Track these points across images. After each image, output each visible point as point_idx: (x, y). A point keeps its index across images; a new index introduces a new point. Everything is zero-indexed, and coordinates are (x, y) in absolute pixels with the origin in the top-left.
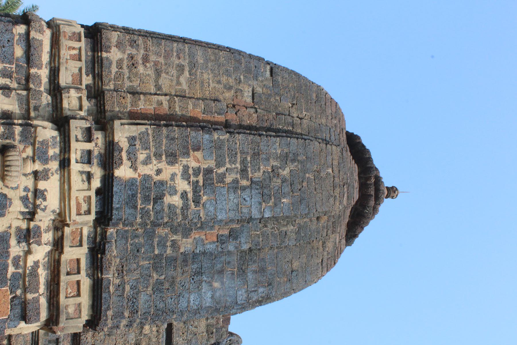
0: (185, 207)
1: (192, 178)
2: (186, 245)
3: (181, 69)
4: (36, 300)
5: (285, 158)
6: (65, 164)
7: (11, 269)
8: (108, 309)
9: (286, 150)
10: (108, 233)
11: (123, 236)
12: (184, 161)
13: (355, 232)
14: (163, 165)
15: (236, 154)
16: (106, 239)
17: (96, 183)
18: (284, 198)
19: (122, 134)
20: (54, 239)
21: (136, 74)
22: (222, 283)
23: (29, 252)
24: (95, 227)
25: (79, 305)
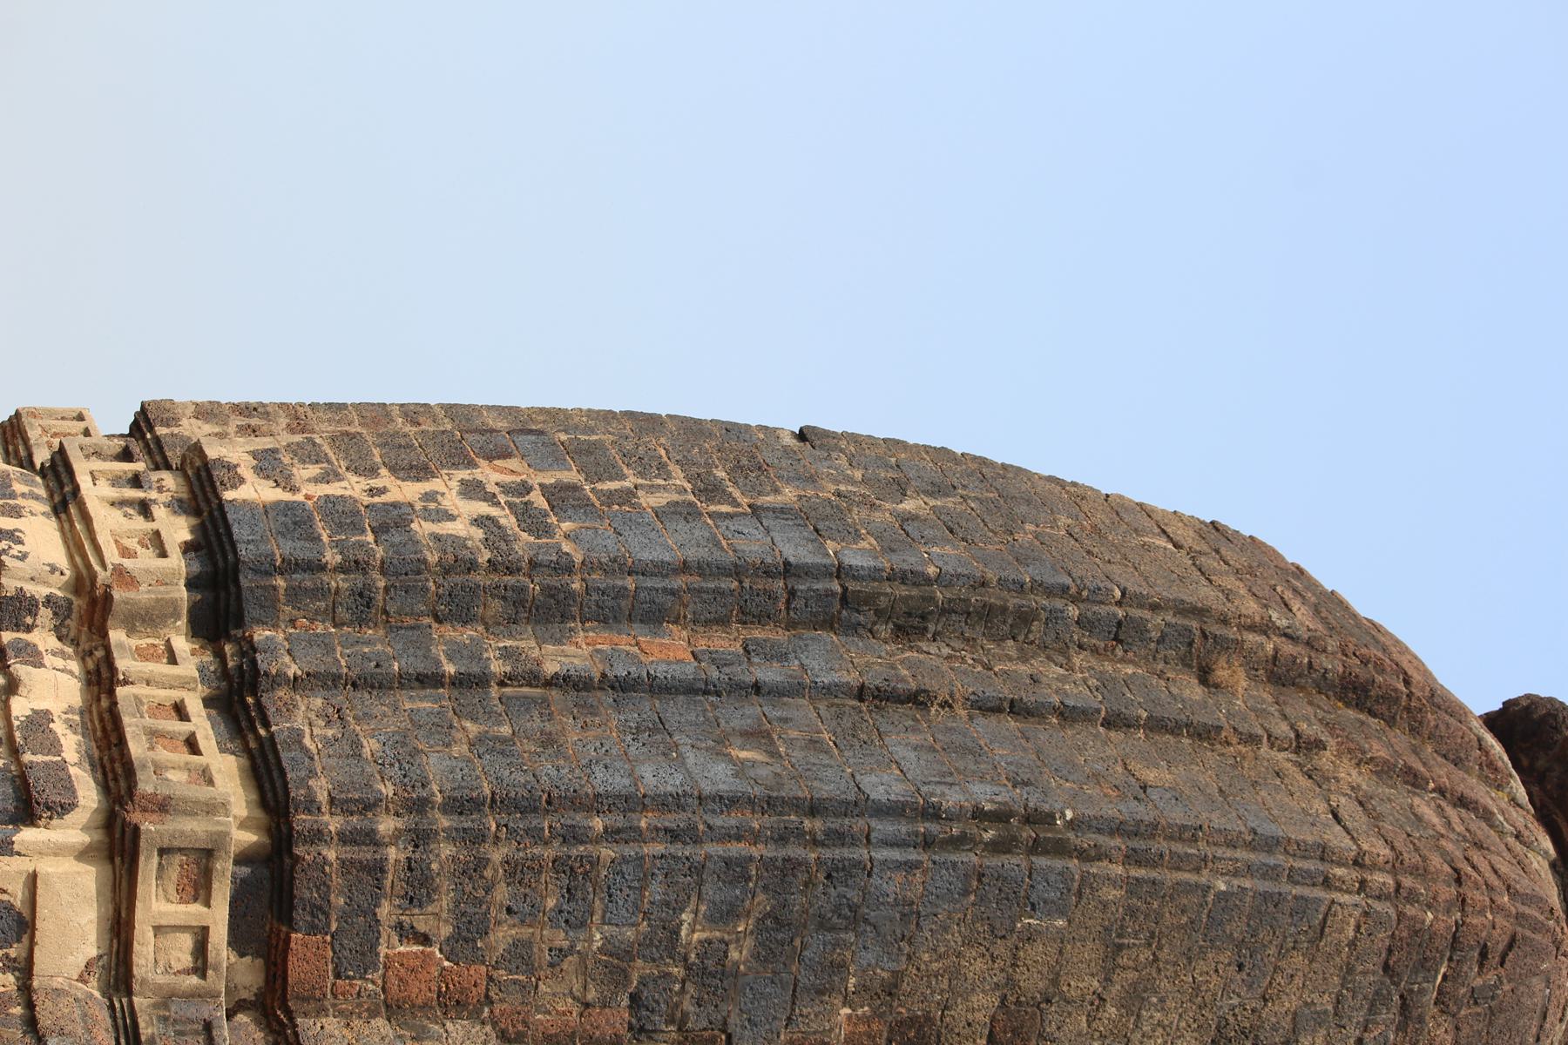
1: (502, 499)
8: (312, 773)
10: (256, 638)
12: (464, 474)
14: (385, 479)
15: (662, 467)
16: (255, 650)
20: (88, 672)
24: (220, 655)
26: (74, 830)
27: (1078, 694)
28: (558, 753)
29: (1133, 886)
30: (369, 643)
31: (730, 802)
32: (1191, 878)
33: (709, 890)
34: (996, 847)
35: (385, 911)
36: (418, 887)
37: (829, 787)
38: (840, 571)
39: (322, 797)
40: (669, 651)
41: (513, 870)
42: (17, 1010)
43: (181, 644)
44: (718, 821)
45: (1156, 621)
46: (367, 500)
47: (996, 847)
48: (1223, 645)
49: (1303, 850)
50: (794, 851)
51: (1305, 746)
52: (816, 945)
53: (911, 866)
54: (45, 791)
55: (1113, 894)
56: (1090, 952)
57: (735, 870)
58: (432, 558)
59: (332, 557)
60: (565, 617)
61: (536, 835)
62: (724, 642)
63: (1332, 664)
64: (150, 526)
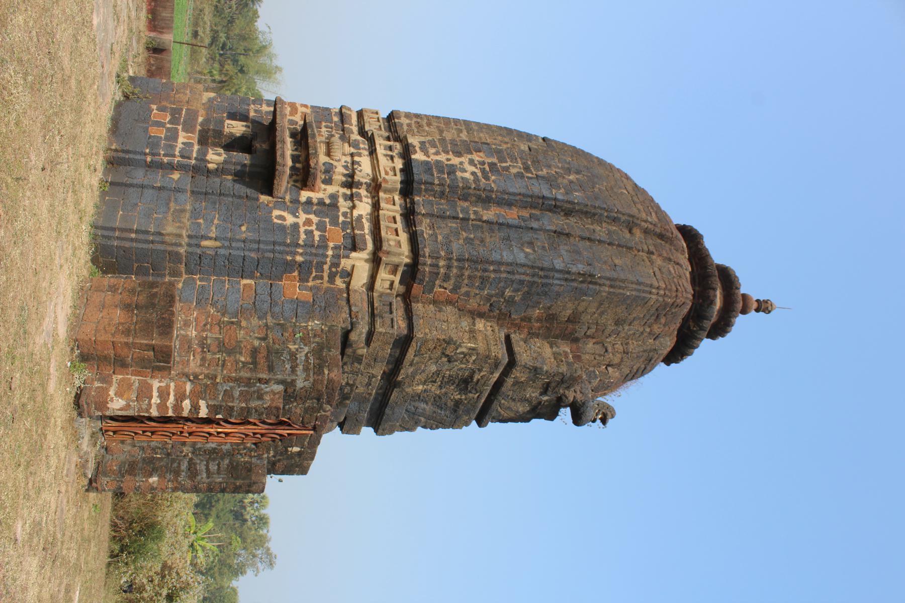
0: (476, 180)
2: (489, 214)
3: (461, 131)
4: (364, 235)
5: (569, 171)
6: (372, 152)
7: (341, 219)
8: (425, 247)
9: (567, 166)
11: (431, 203)
12: (469, 156)
13: (709, 296)
14: (451, 156)
17: (399, 164)
18: (576, 191)
19: (413, 140)
21: (424, 131)
22: (534, 250)
23: (354, 207)
25: (399, 242)
26: (365, 255)
27: (604, 236)
28: (484, 246)
29: (609, 293)
30: (442, 204)
31: (523, 265)
32: (621, 291)
33: (514, 286)
34: (582, 282)
35: (437, 282)
36: (447, 278)
37: (546, 264)
38: (555, 199)
39: (427, 255)
40: (512, 215)
41: (470, 277)
42: (345, 295)
43: (397, 198)
44: (519, 270)
45: (623, 218)
46: (446, 163)
47: (582, 282)
48: (637, 225)
49: (647, 285)
50: (536, 279)
51: (650, 253)
52: (535, 298)
53: (561, 285)
54: (360, 245)
55: (604, 294)
56: (596, 304)
57: (521, 282)
58: (461, 185)
59: (437, 182)
60: (489, 202)
61: (476, 269)
62: (525, 213)
63: (658, 230)
64: (393, 165)
